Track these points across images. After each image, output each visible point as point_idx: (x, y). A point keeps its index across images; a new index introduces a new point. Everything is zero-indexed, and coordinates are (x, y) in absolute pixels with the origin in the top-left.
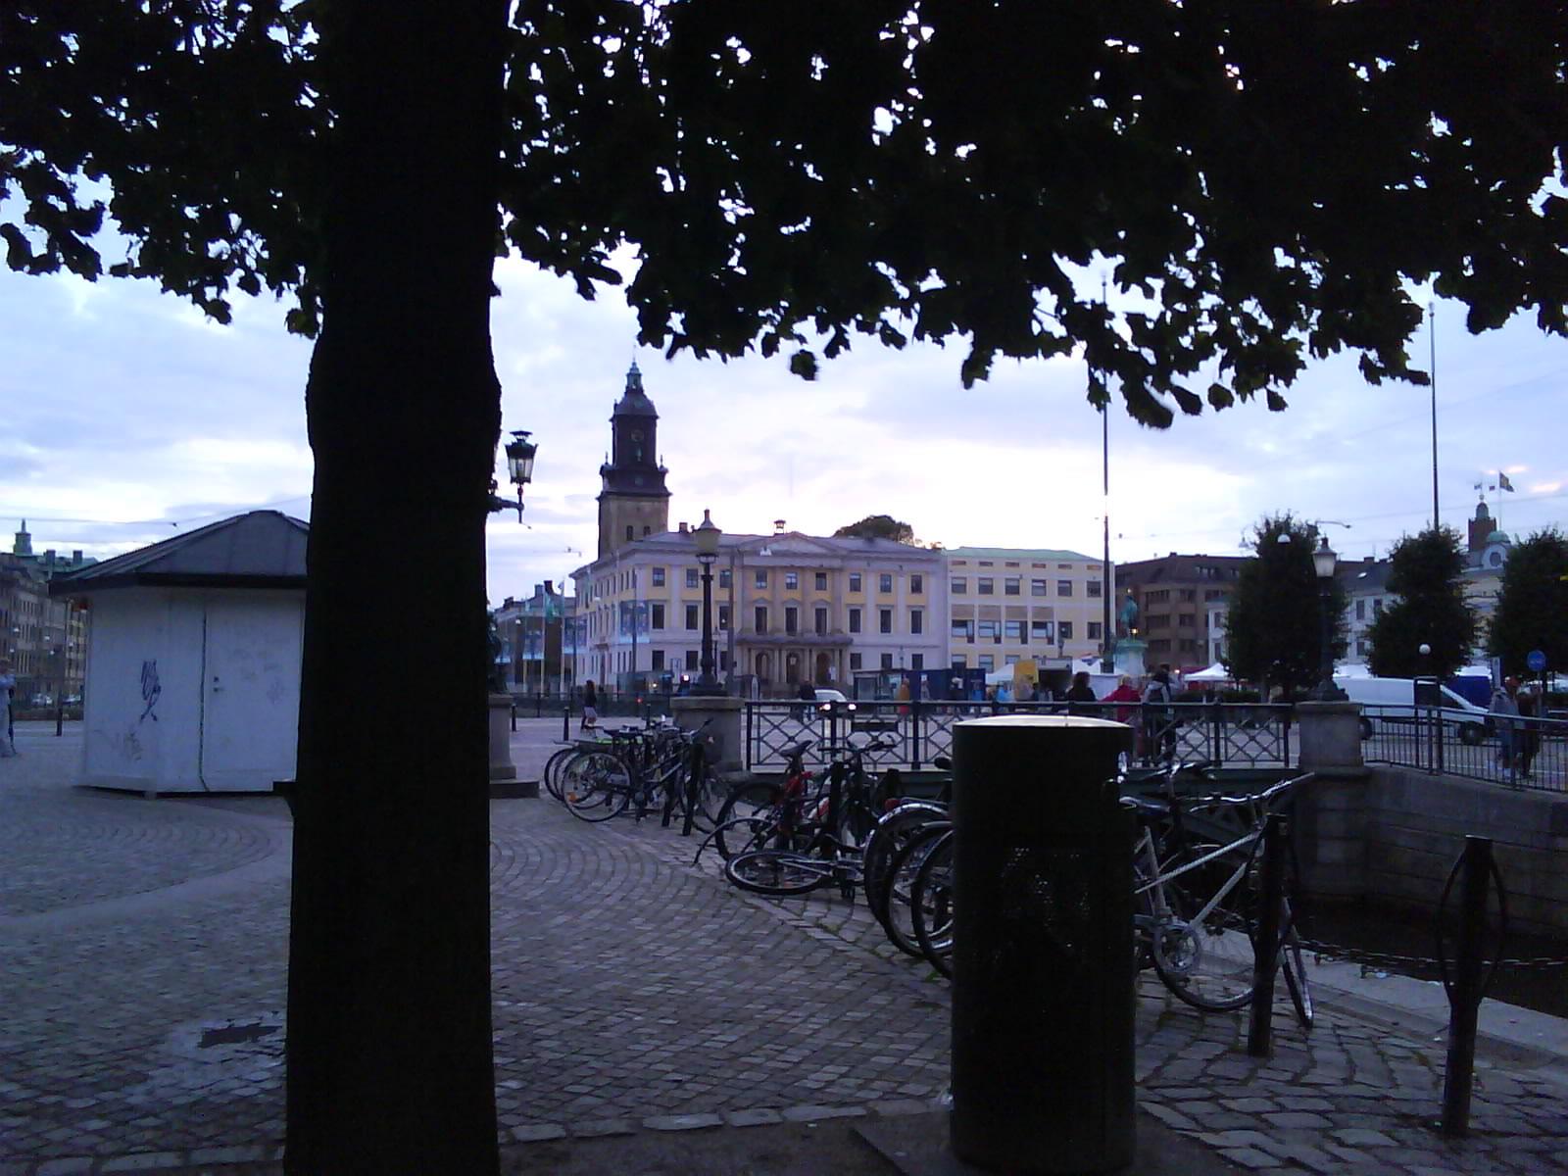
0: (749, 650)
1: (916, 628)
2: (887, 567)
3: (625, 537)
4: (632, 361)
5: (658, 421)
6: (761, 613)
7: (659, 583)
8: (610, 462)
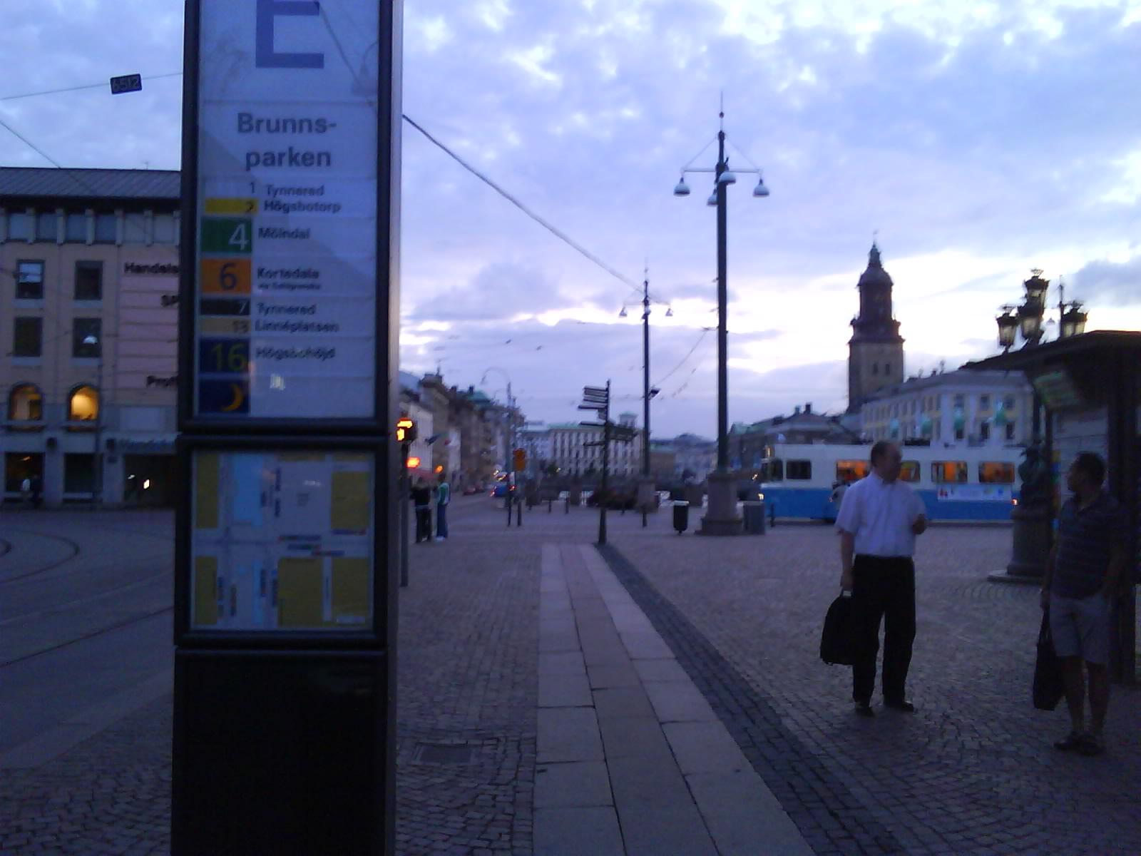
4: (872, 244)
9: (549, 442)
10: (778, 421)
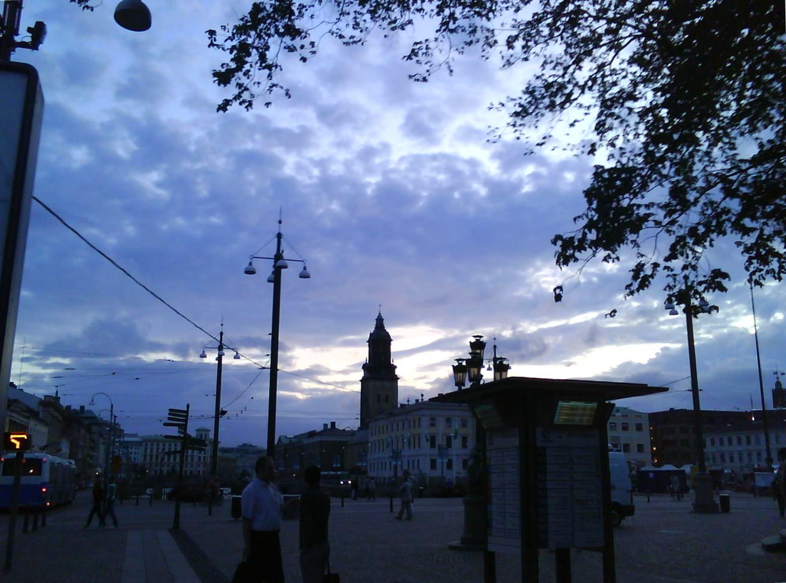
4: (378, 313)
5: (392, 342)
7: (433, 425)
8: (368, 362)
9: (142, 449)
10: (312, 434)
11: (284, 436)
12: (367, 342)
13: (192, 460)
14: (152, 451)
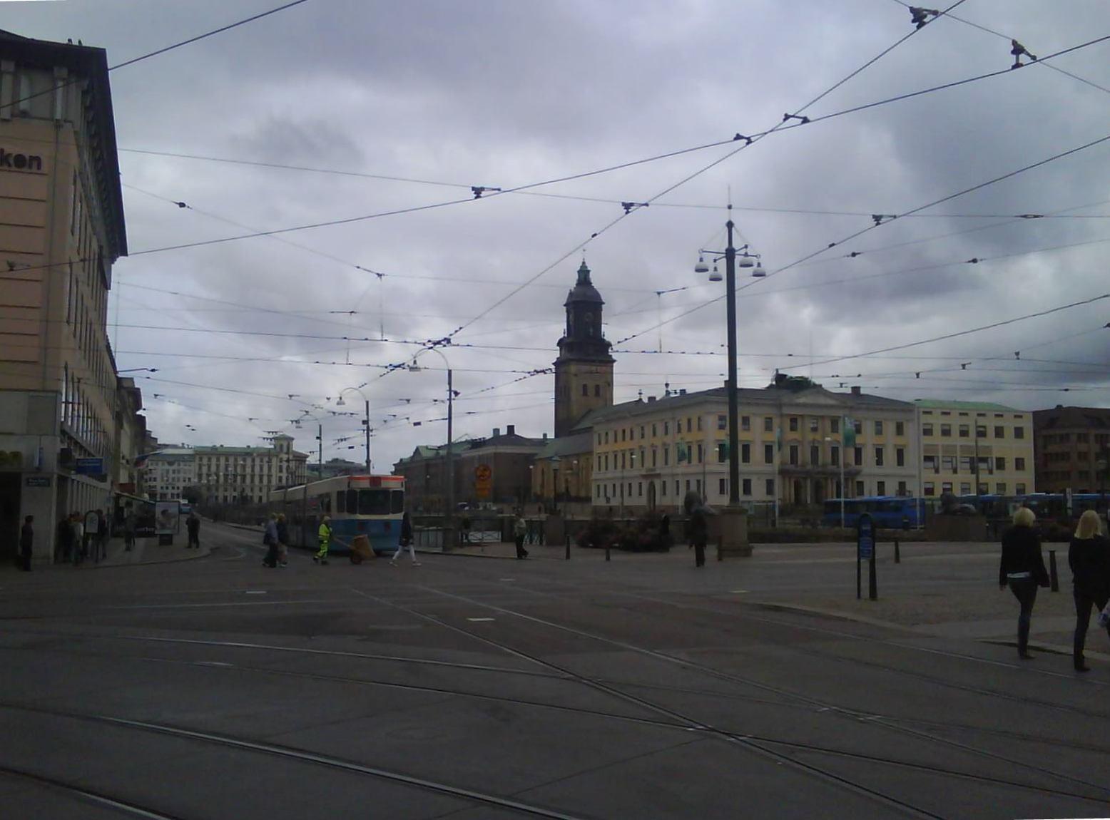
0: (790, 478)
1: (900, 462)
2: (880, 416)
3: (582, 393)
4: (582, 261)
5: (603, 306)
6: (794, 450)
8: (566, 335)
9: (194, 467)
11: (424, 447)
12: (565, 305)
13: (261, 480)
14: (253, 470)
